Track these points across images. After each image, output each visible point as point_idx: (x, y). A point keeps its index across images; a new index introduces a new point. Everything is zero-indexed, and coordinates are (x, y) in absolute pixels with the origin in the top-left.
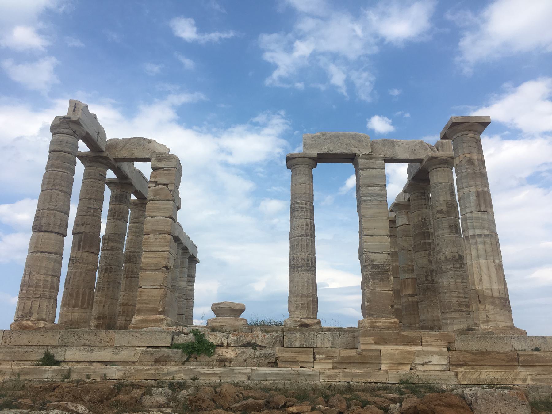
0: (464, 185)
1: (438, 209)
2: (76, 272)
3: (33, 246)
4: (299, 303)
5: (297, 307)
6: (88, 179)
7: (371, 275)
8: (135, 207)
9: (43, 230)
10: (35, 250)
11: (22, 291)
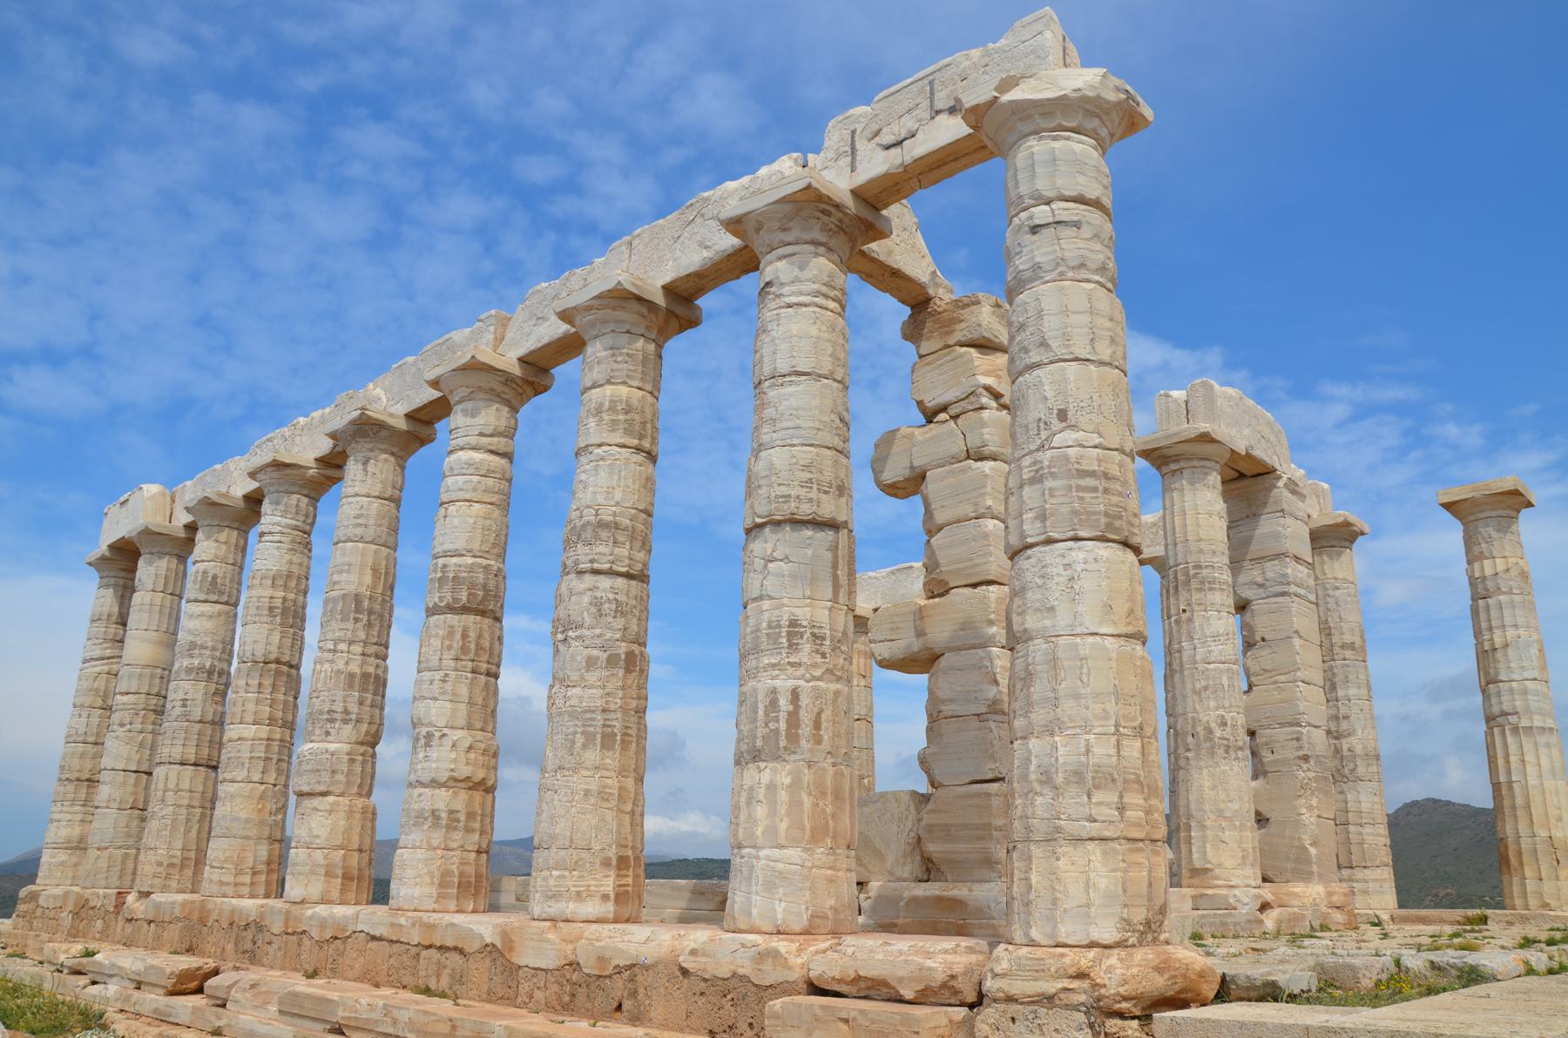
0: (1520, 621)
1: (1348, 638)
2: (837, 693)
3: (1121, 607)
4: (1249, 846)
5: (1244, 858)
6: (826, 296)
7: (1316, 779)
8: (499, 388)
9: (1135, 540)
10: (1130, 630)
11: (1121, 809)
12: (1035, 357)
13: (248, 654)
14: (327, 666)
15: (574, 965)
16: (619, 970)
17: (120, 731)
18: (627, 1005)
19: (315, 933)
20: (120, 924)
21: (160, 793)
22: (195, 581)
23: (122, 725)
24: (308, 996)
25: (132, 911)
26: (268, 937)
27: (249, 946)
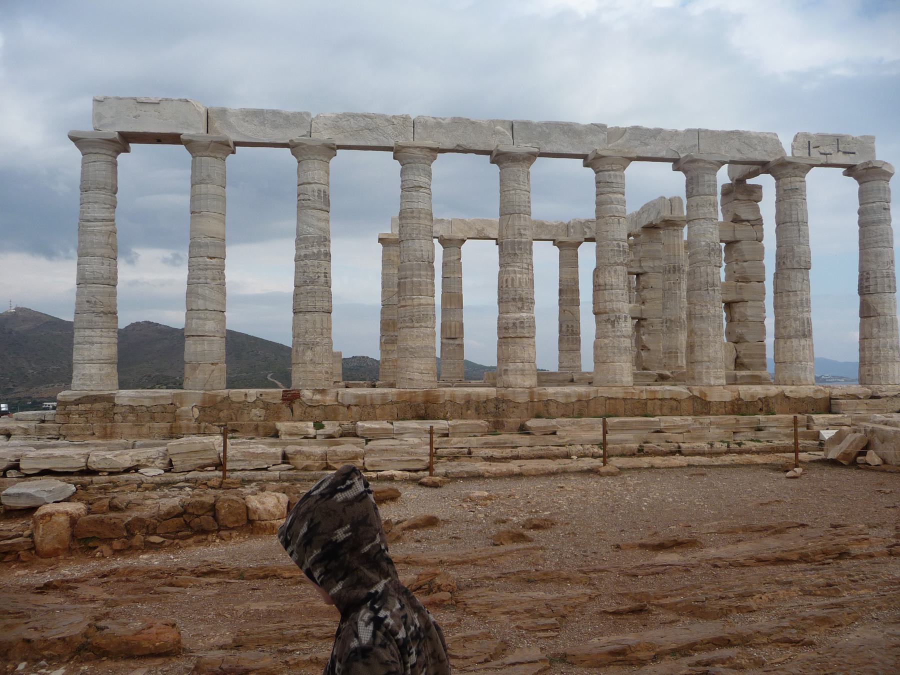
12: (886, 245)
13: (425, 257)
14: (525, 276)
15: (739, 399)
16: (759, 399)
17: (213, 284)
18: (764, 409)
19: (561, 400)
20: (298, 411)
21: (319, 330)
22: (319, 196)
23: (214, 279)
24: (635, 422)
25: (318, 401)
26: (512, 405)
27: (493, 410)
